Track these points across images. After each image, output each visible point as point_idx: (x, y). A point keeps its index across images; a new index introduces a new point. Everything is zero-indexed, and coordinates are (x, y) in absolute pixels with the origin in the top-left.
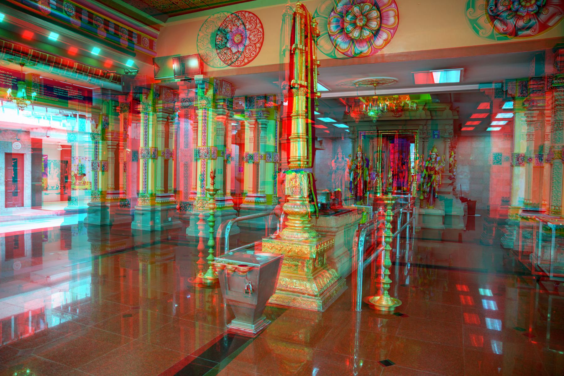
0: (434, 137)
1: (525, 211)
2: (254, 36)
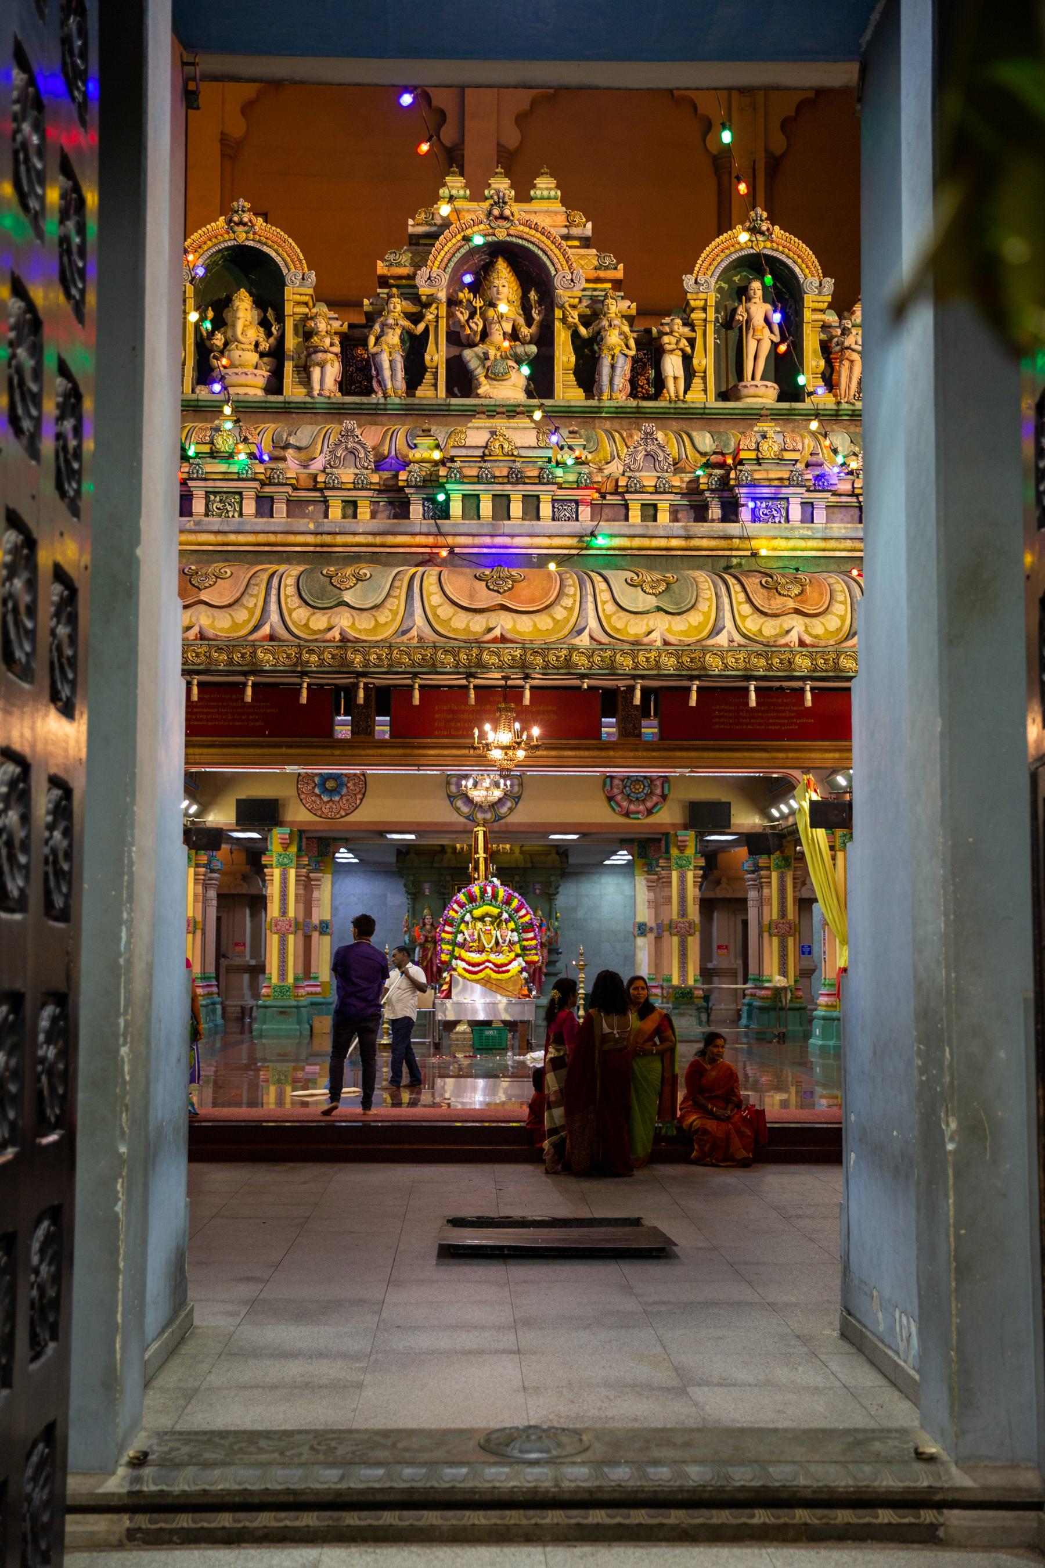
0: (535, 893)
2: (354, 784)
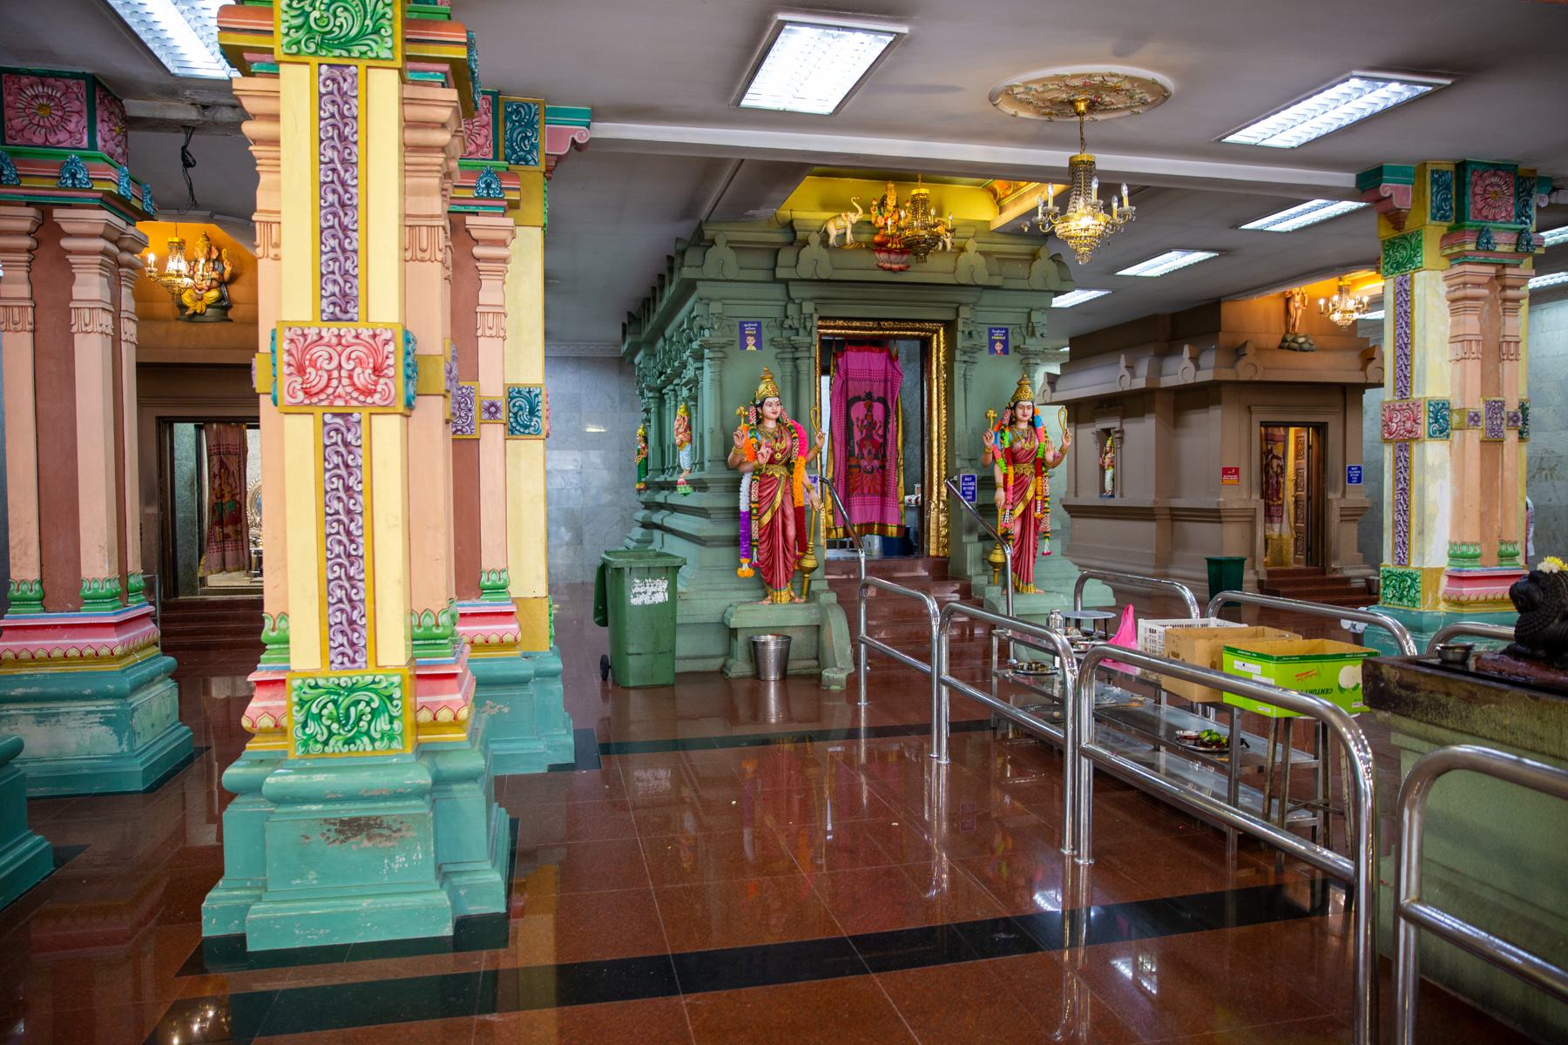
0: (992, 350)
1: (1456, 579)
